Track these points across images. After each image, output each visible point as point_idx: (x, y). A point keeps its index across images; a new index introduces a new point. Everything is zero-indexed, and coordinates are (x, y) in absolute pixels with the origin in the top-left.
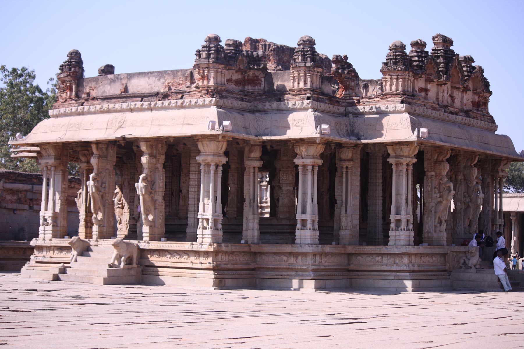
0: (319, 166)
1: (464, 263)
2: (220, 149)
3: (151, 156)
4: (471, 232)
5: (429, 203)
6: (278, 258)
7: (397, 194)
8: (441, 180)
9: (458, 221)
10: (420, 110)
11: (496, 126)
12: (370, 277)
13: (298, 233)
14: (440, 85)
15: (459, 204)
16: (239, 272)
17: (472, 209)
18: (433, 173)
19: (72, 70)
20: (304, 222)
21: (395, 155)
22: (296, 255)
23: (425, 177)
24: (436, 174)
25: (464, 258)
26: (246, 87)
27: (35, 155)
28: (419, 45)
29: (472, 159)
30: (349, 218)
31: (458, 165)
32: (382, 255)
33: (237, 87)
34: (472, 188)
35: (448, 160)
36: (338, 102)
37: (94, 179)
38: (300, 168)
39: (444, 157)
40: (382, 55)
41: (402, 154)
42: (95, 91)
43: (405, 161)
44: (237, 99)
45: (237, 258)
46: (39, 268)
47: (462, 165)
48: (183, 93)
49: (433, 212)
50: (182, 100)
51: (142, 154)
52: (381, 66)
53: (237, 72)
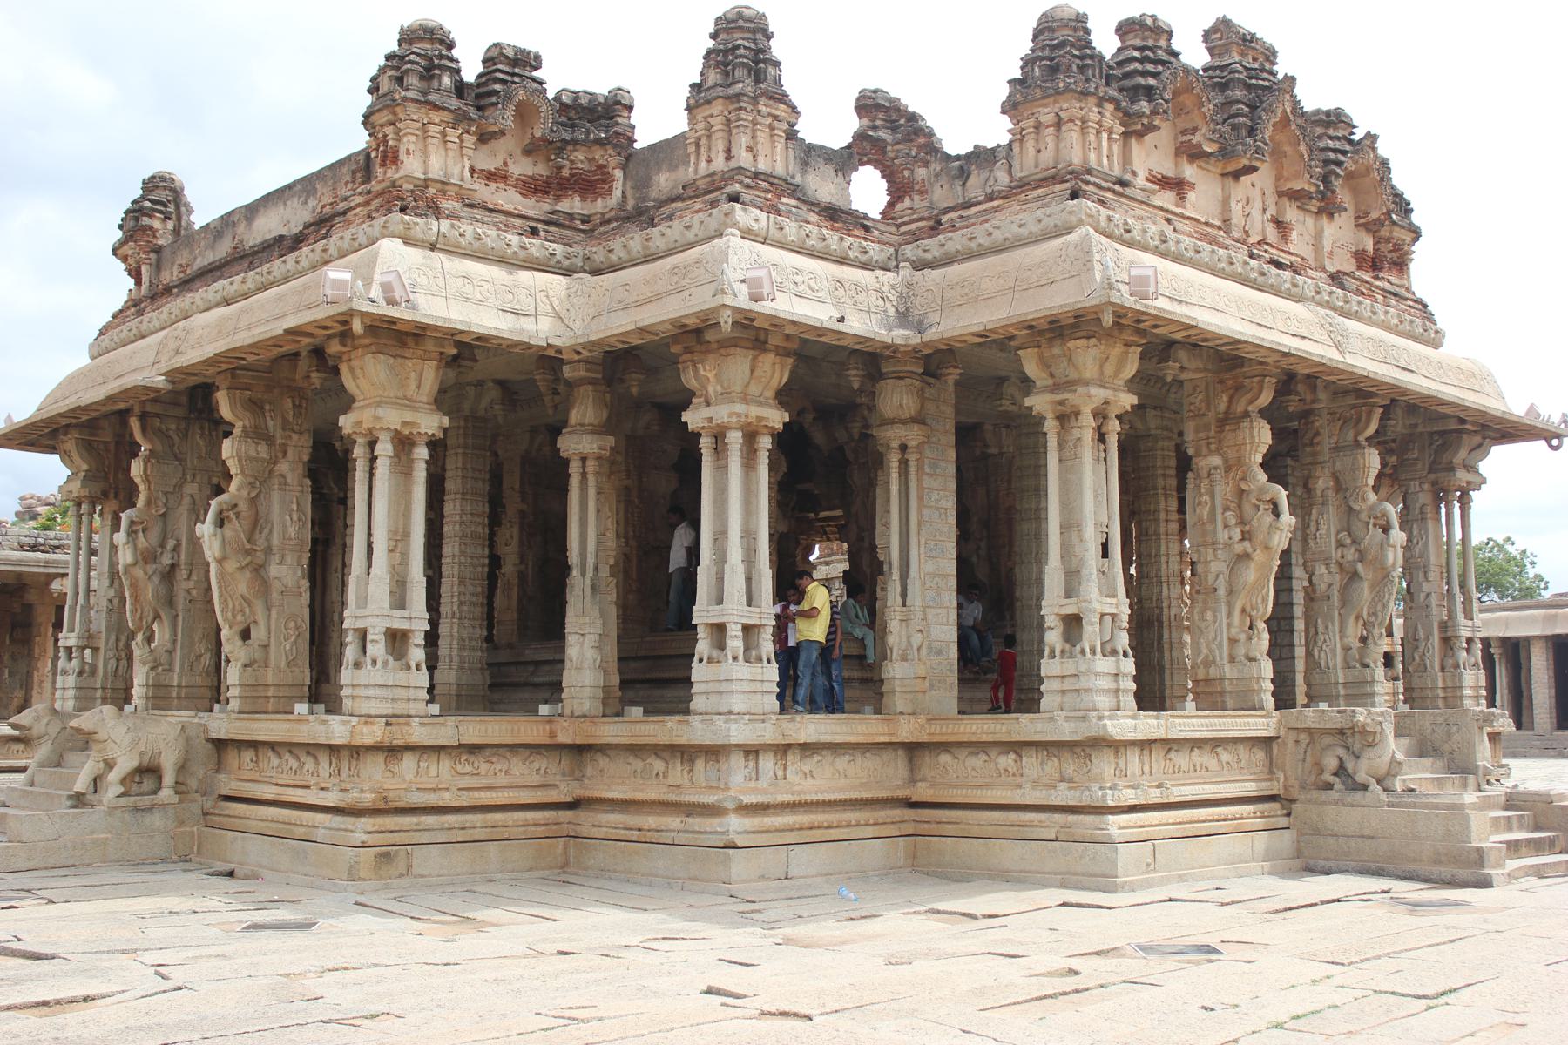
1: (1341, 771)
2: (413, 386)
4: (1367, 661)
5: (1207, 562)
6: (638, 764)
8: (1244, 479)
9: (1321, 628)
12: (975, 831)
13: (698, 672)
15: (1323, 570)
16: (498, 817)
17: (1366, 585)
20: (719, 629)
21: (1050, 382)
23: (1190, 475)
24: (1226, 461)
25: (1341, 752)
28: (1145, 35)
29: (1359, 420)
31: (1312, 444)
32: (1017, 747)
33: (531, 202)
34: (1364, 516)
35: (1264, 413)
36: (867, 229)
38: (705, 443)
39: (1252, 402)
41: (1073, 375)
45: (498, 767)
47: (1327, 442)
49: (1222, 592)
52: (1004, 92)
53: (527, 152)
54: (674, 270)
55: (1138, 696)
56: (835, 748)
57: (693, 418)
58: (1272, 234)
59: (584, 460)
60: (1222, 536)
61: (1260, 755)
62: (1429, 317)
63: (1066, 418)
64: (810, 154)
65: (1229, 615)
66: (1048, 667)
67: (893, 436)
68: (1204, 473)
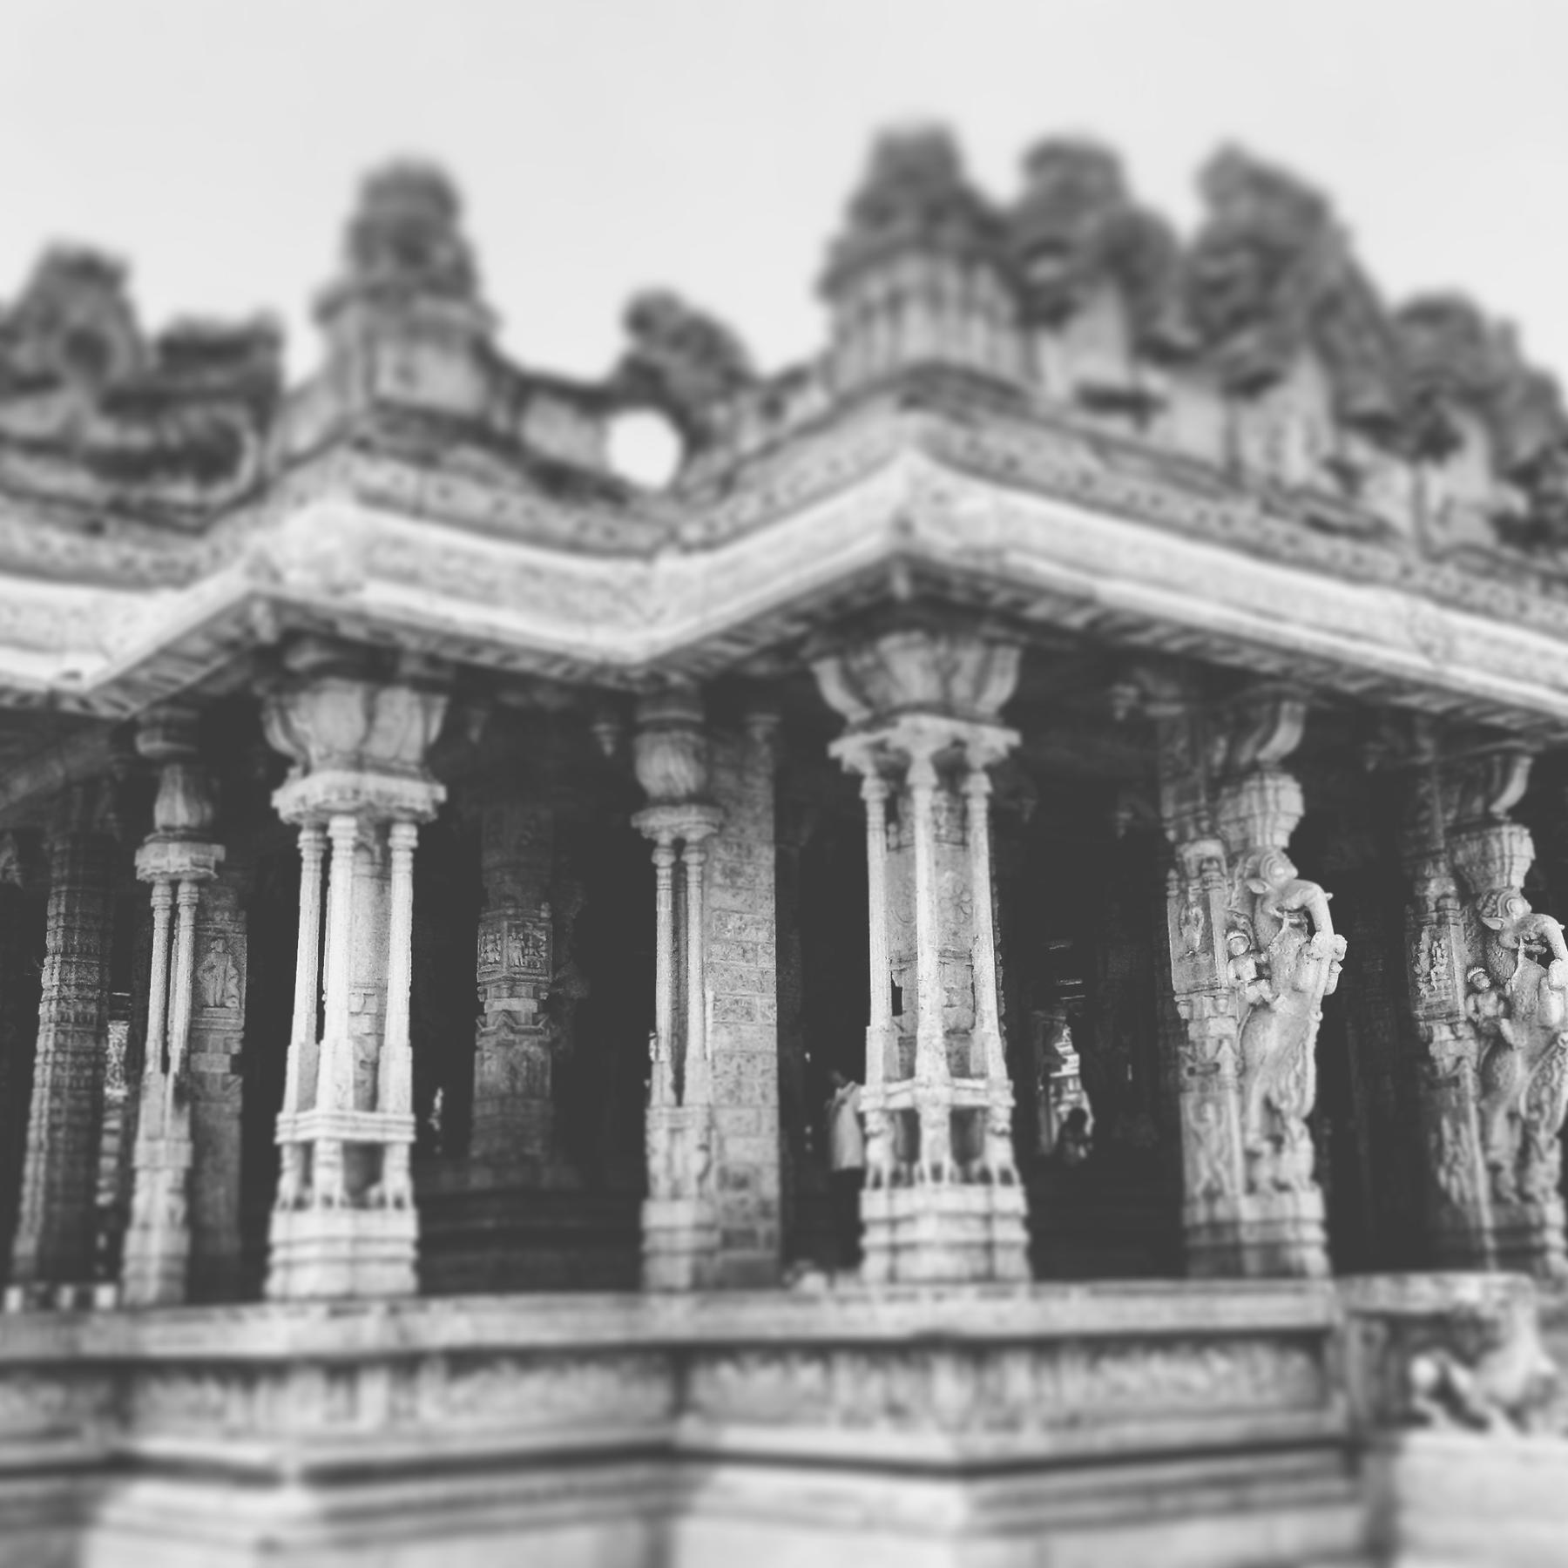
0: (418, 821)
1: (1444, 1392)
5: (1203, 1021)
8: (1255, 875)
24: (1226, 844)
29: (1489, 780)
34: (1507, 940)
47: (1443, 819)
49: (1228, 1070)
56: (527, 1358)
58: (1327, 483)
59: (174, 884)
60: (1225, 973)
61: (1298, 1362)
64: (526, 388)
65: (1243, 1109)
67: (661, 824)
68: (1192, 869)
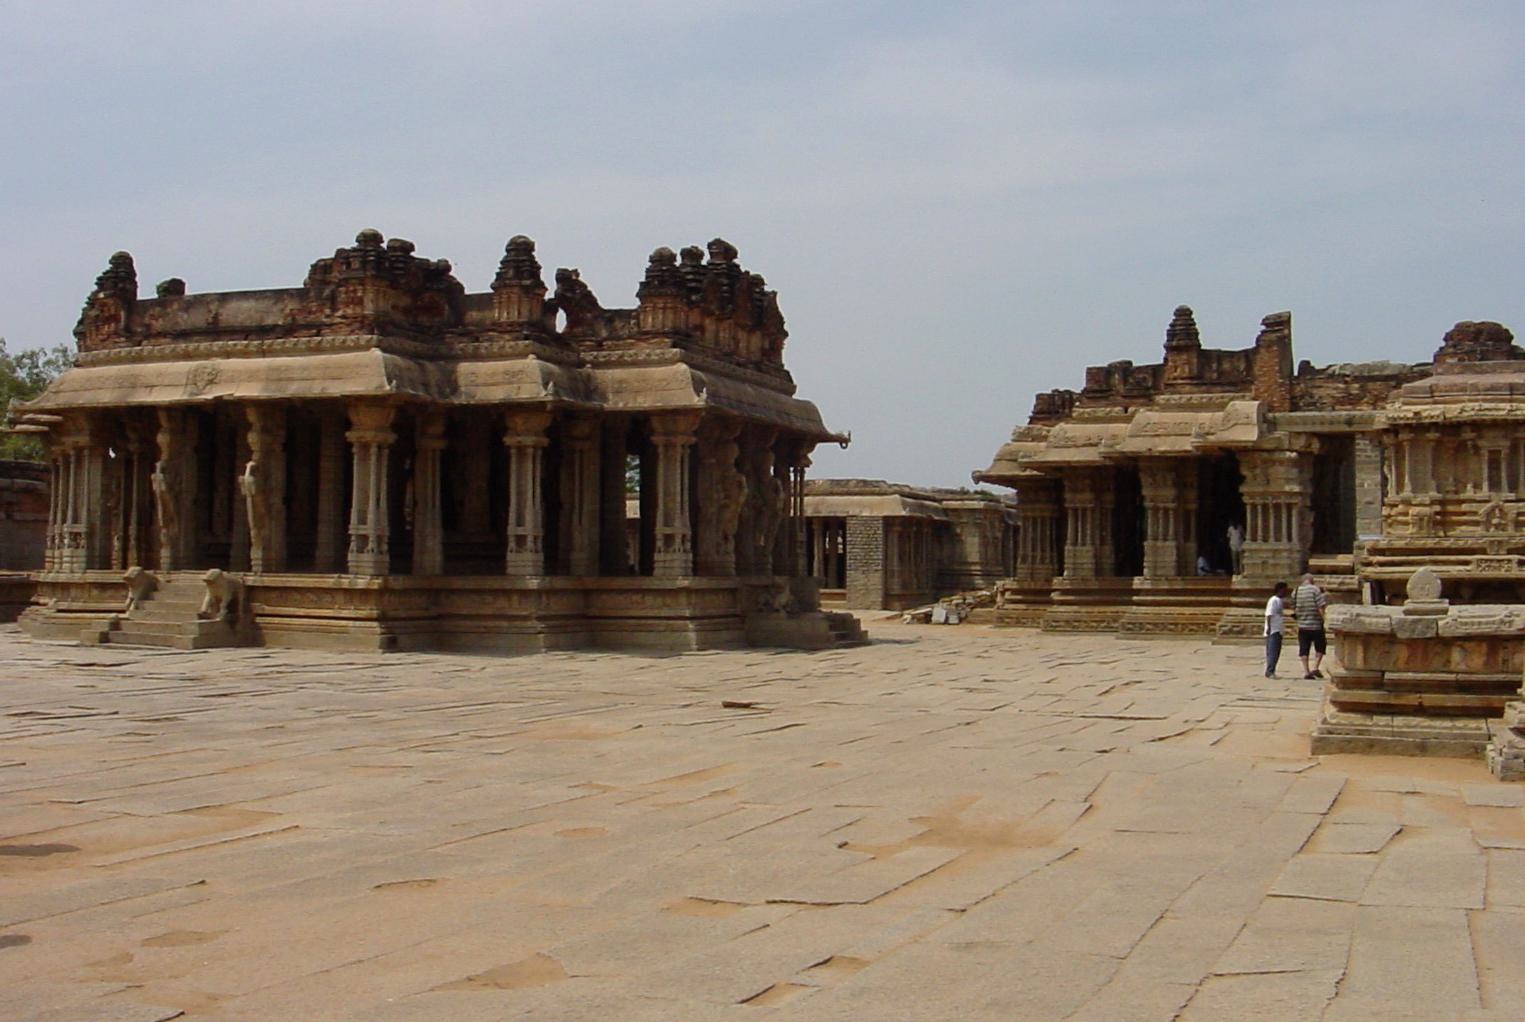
1: (766, 604)
3: (265, 430)
7: (667, 494)
10: (698, 359)
11: (795, 387)
13: (510, 556)
14: (720, 320)
18: (713, 461)
19: (120, 285)
22: (507, 593)
26: (419, 319)
27: (46, 428)
28: (691, 254)
30: (583, 536)
37: (163, 471)
40: (638, 272)
42: (161, 321)
43: (680, 440)
44: (408, 338)
46: (64, 621)
48: (320, 326)
50: (319, 338)
51: (249, 427)
54: (506, 373)
55: (736, 569)
57: (508, 440)
60: (715, 496)
62: (791, 380)
63: (669, 446)
66: (657, 557)
